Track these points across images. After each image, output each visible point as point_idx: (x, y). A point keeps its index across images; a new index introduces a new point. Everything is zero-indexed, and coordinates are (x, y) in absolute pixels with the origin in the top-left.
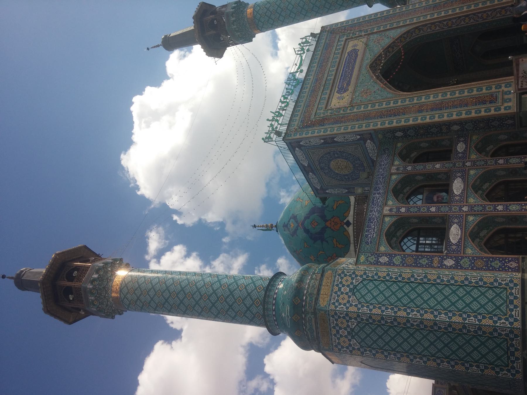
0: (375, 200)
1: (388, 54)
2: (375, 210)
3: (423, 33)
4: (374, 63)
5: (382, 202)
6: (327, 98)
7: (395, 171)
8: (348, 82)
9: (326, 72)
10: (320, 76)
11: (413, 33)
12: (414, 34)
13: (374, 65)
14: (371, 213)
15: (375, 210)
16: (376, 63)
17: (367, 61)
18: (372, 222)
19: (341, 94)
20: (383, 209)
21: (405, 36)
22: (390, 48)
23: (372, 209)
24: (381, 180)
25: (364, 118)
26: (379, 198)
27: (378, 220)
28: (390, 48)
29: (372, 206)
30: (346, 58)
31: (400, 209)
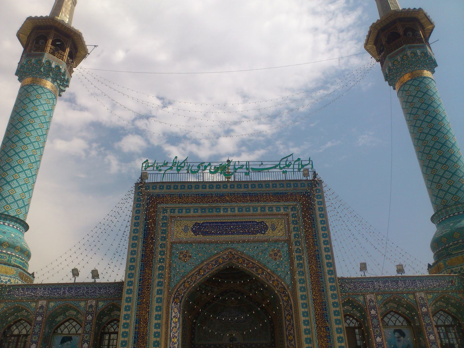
0: (58, 290)
1: (254, 269)
2: (45, 292)
3: (284, 306)
4: (238, 256)
5: (53, 298)
6: (189, 214)
7: (89, 304)
8: (209, 233)
9: (233, 203)
10: (227, 198)
11: (284, 295)
12: (283, 295)
13: (236, 257)
14: (42, 289)
15: (45, 292)
16: (238, 258)
17: (239, 247)
18: (32, 292)
19: (192, 229)
20: (45, 299)
21: (280, 286)
22: (261, 270)
23: (47, 289)
24: (80, 292)
25: (146, 261)
26: (58, 293)
27: (34, 297)
28: (261, 270)
29: (51, 289)
30: (253, 222)
31: (41, 316)
